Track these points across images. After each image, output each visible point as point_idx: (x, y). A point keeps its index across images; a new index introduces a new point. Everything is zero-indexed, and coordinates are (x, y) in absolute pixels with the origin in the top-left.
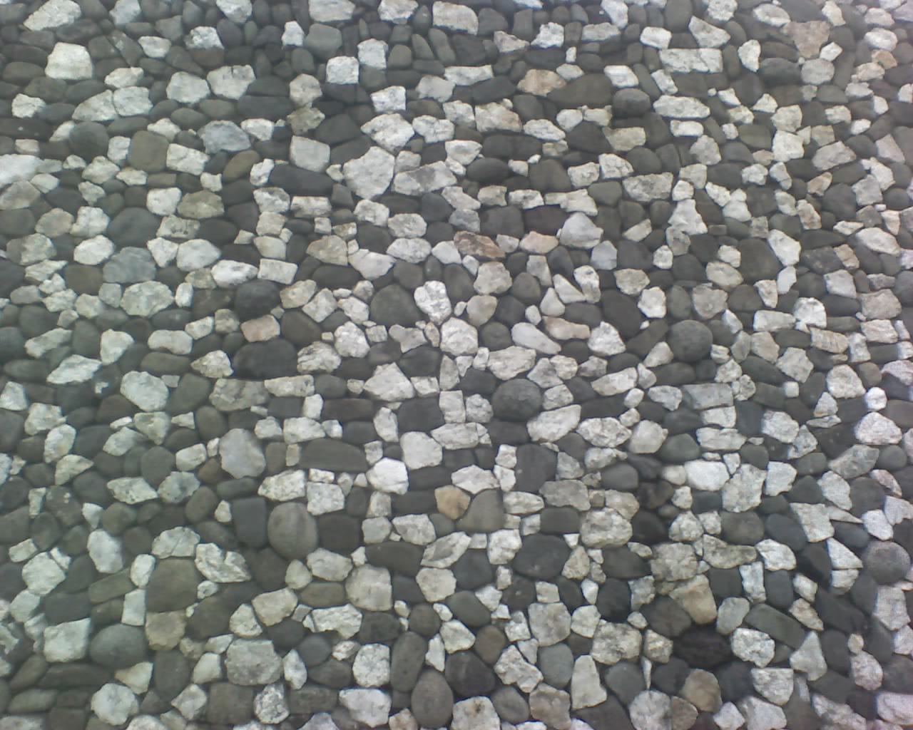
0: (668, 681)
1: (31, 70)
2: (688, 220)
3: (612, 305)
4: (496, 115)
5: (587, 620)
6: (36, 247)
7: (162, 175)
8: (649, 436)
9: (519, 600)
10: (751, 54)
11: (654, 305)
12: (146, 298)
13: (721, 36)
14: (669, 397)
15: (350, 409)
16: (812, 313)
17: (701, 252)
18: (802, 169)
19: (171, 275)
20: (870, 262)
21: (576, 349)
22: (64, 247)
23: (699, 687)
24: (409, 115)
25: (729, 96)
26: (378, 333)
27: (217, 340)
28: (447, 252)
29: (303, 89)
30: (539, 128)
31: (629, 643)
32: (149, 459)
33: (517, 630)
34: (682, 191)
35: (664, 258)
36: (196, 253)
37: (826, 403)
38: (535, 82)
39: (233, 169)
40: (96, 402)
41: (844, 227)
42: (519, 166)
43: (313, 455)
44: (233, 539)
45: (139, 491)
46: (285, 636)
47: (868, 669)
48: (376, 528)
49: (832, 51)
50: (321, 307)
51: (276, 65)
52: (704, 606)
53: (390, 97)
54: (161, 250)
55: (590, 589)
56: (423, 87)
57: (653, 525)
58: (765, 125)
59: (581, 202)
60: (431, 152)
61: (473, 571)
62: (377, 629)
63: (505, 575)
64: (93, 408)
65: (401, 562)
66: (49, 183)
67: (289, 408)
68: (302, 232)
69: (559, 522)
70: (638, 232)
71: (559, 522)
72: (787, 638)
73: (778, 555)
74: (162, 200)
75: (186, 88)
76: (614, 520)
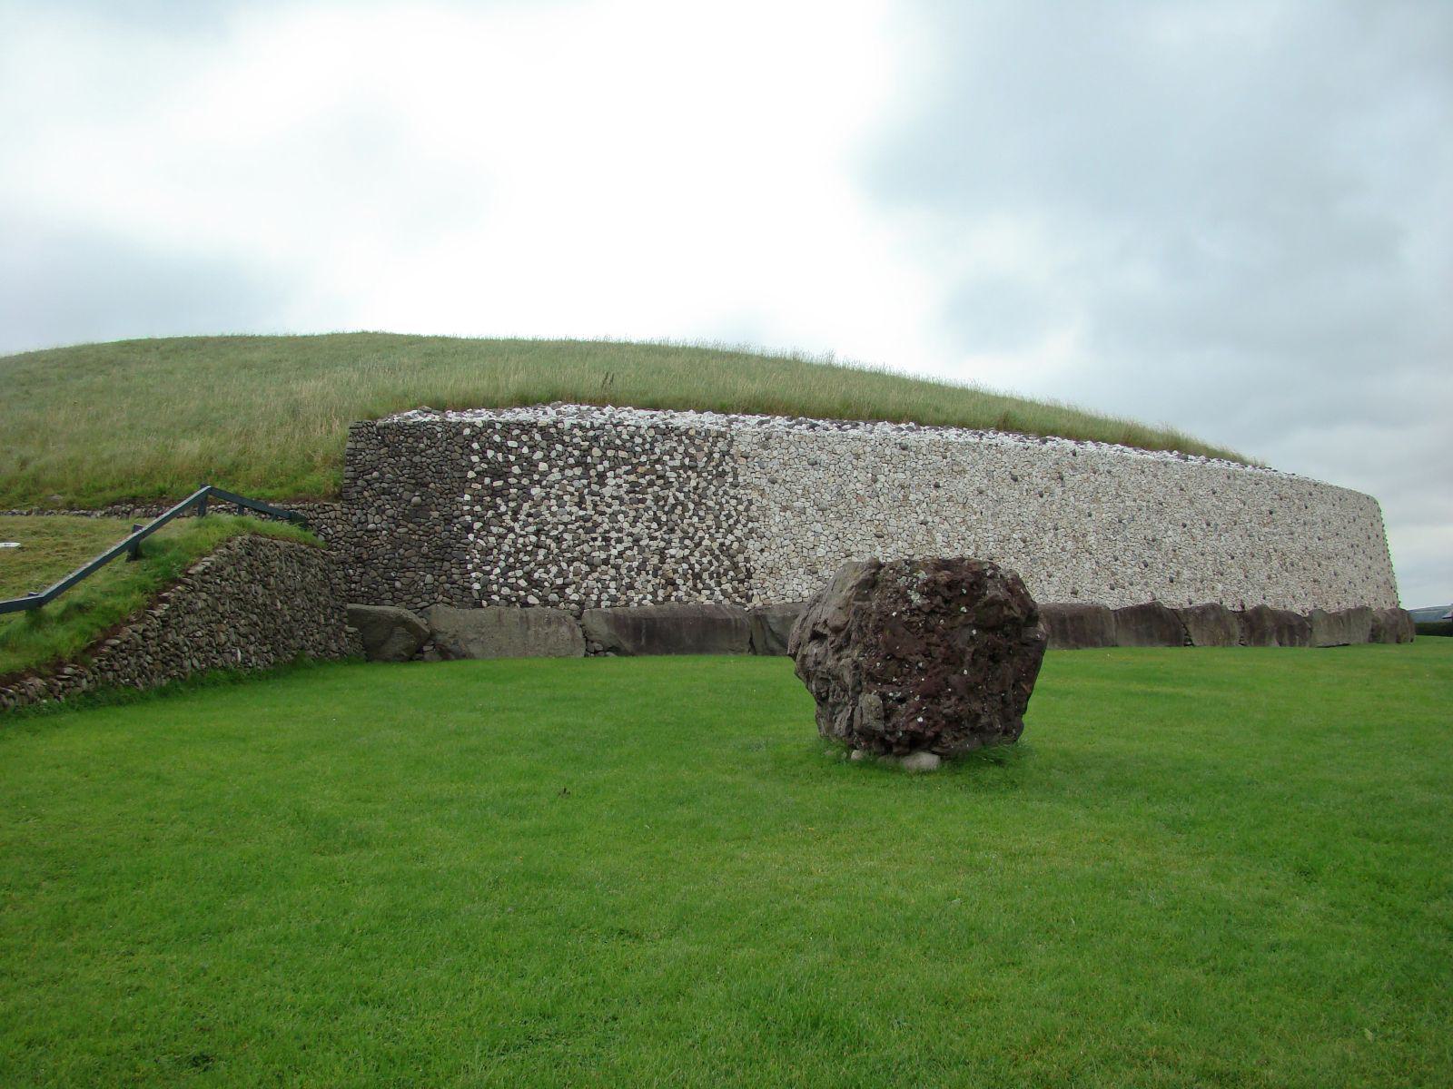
0: (664, 588)
1: (536, 469)
2: (671, 500)
3: (656, 519)
4: (632, 478)
5: (650, 577)
6: (543, 508)
7: (566, 492)
8: (662, 544)
9: (638, 574)
10: (687, 461)
11: (664, 518)
12: (566, 518)
13: (681, 457)
14: (666, 537)
15: (606, 539)
16: (695, 519)
17: (674, 507)
18: (696, 488)
19: (570, 514)
20: (709, 508)
21: (649, 528)
22: (549, 508)
23: (670, 588)
24: (614, 478)
25: (681, 471)
26: (611, 525)
27: (581, 527)
28: (623, 508)
29: (593, 473)
30: (641, 481)
31: (657, 581)
32: (570, 549)
33: (638, 579)
34: (671, 494)
35: (666, 509)
36: (575, 509)
37: (697, 537)
38: (640, 470)
39: (580, 491)
40: (558, 539)
41: (703, 501)
42: (637, 489)
43: (600, 548)
44: (587, 564)
45: (569, 555)
46: (598, 580)
47: (700, 586)
48: (612, 561)
49: (705, 459)
50: (599, 519)
51: (587, 467)
52: (671, 575)
53: (610, 474)
54: (568, 508)
55: (650, 572)
56: (617, 471)
57: (662, 561)
58: (688, 477)
59: (649, 497)
60: (620, 486)
61: (630, 569)
62: (613, 579)
63: (636, 570)
64: (559, 540)
65: (617, 567)
66: (544, 494)
67: (594, 539)
68: (595, 505)
69: (645, 561)
70: (661, 503)
71: (645, 561)
72: (686, 580)
73: (685, 566)
74: (566, 498)
75: (568, 473)
76: (655, 560)
